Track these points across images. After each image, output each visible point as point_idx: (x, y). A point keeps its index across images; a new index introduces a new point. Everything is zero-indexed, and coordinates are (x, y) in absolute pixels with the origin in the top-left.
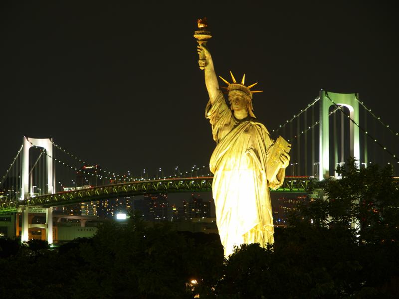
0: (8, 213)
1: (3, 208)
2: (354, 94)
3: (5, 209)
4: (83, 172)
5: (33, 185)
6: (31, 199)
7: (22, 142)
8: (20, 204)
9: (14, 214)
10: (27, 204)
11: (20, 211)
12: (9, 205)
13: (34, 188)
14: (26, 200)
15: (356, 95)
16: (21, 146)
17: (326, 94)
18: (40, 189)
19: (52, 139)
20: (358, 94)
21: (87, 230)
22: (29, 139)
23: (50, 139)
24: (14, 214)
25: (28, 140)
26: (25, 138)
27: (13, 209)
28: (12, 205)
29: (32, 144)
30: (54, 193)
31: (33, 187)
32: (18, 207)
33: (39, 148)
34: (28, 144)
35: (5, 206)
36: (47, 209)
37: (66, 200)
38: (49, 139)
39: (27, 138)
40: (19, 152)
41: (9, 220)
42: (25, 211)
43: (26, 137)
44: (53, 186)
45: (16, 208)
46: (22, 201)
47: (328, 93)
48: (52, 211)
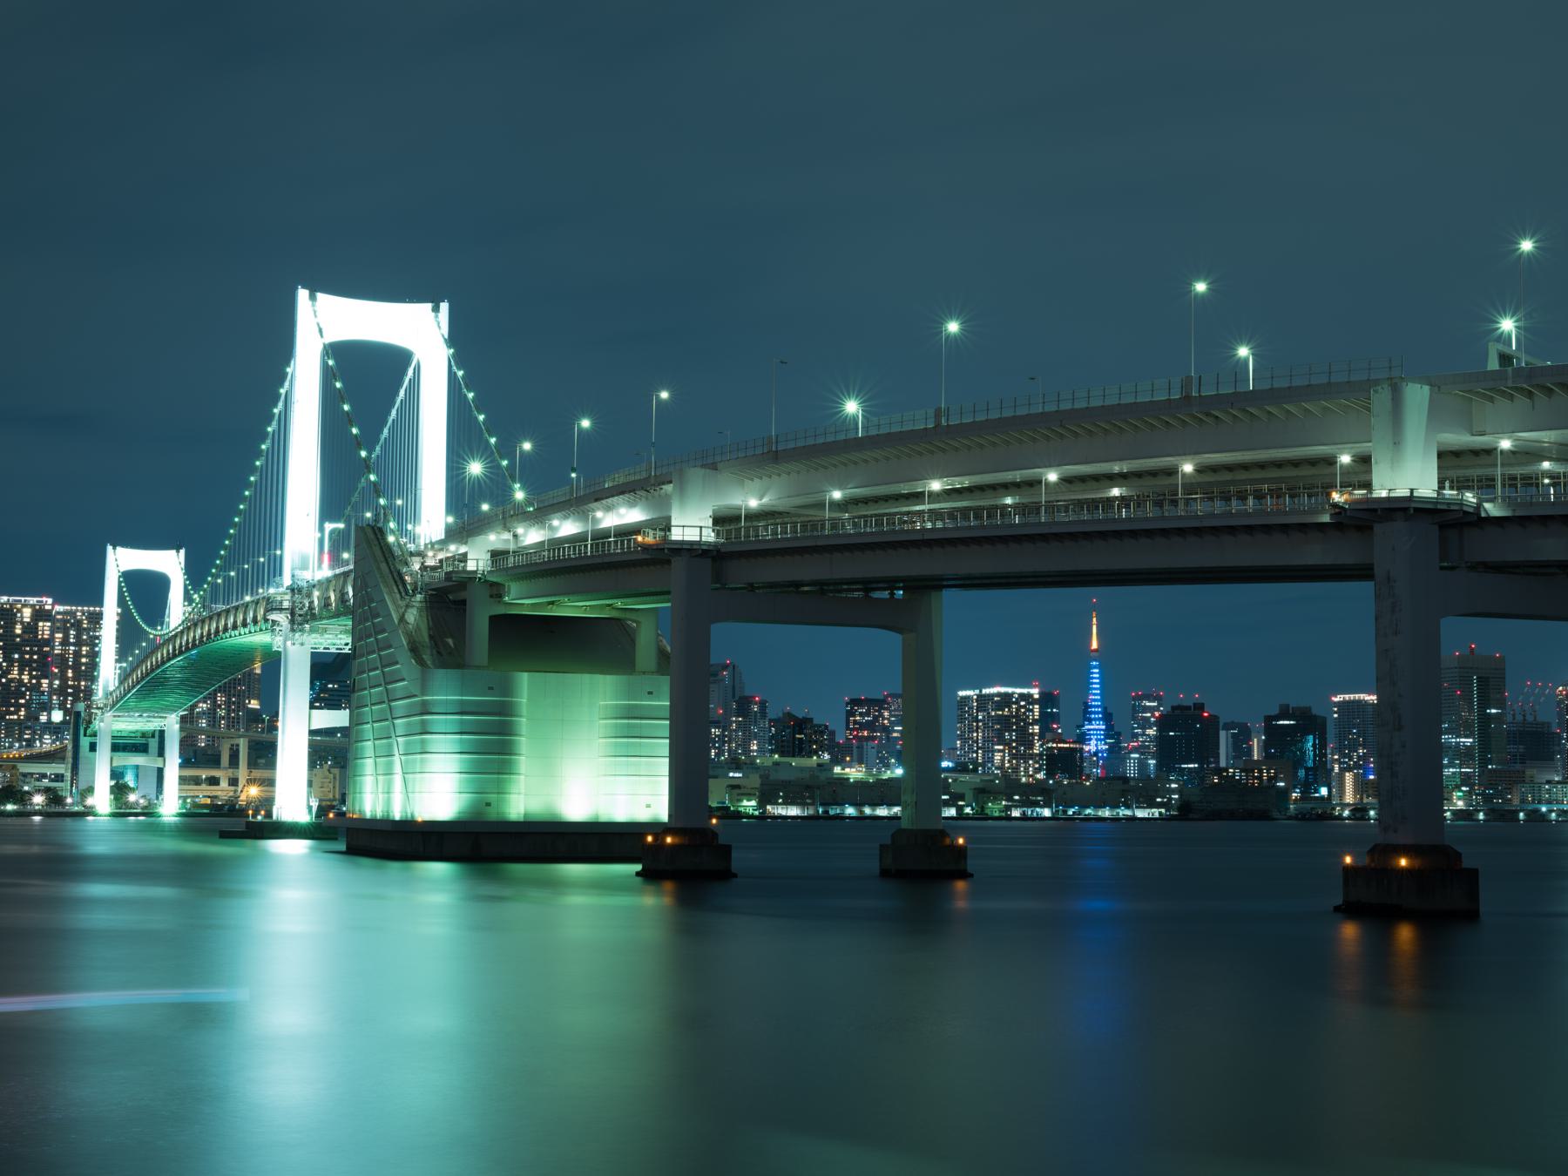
0: (144, 735)
2: (429, 306)
13: (120, 668)
15: (436, 309)
17: (313, 297)
19: (182, 552)
20: (444, 307)
23: (178, 552)
24: (157, 734)
34: (121, 560)
39: (114, 548)
42: (102, 724)
47: (319, 295)
48: (177, 726)
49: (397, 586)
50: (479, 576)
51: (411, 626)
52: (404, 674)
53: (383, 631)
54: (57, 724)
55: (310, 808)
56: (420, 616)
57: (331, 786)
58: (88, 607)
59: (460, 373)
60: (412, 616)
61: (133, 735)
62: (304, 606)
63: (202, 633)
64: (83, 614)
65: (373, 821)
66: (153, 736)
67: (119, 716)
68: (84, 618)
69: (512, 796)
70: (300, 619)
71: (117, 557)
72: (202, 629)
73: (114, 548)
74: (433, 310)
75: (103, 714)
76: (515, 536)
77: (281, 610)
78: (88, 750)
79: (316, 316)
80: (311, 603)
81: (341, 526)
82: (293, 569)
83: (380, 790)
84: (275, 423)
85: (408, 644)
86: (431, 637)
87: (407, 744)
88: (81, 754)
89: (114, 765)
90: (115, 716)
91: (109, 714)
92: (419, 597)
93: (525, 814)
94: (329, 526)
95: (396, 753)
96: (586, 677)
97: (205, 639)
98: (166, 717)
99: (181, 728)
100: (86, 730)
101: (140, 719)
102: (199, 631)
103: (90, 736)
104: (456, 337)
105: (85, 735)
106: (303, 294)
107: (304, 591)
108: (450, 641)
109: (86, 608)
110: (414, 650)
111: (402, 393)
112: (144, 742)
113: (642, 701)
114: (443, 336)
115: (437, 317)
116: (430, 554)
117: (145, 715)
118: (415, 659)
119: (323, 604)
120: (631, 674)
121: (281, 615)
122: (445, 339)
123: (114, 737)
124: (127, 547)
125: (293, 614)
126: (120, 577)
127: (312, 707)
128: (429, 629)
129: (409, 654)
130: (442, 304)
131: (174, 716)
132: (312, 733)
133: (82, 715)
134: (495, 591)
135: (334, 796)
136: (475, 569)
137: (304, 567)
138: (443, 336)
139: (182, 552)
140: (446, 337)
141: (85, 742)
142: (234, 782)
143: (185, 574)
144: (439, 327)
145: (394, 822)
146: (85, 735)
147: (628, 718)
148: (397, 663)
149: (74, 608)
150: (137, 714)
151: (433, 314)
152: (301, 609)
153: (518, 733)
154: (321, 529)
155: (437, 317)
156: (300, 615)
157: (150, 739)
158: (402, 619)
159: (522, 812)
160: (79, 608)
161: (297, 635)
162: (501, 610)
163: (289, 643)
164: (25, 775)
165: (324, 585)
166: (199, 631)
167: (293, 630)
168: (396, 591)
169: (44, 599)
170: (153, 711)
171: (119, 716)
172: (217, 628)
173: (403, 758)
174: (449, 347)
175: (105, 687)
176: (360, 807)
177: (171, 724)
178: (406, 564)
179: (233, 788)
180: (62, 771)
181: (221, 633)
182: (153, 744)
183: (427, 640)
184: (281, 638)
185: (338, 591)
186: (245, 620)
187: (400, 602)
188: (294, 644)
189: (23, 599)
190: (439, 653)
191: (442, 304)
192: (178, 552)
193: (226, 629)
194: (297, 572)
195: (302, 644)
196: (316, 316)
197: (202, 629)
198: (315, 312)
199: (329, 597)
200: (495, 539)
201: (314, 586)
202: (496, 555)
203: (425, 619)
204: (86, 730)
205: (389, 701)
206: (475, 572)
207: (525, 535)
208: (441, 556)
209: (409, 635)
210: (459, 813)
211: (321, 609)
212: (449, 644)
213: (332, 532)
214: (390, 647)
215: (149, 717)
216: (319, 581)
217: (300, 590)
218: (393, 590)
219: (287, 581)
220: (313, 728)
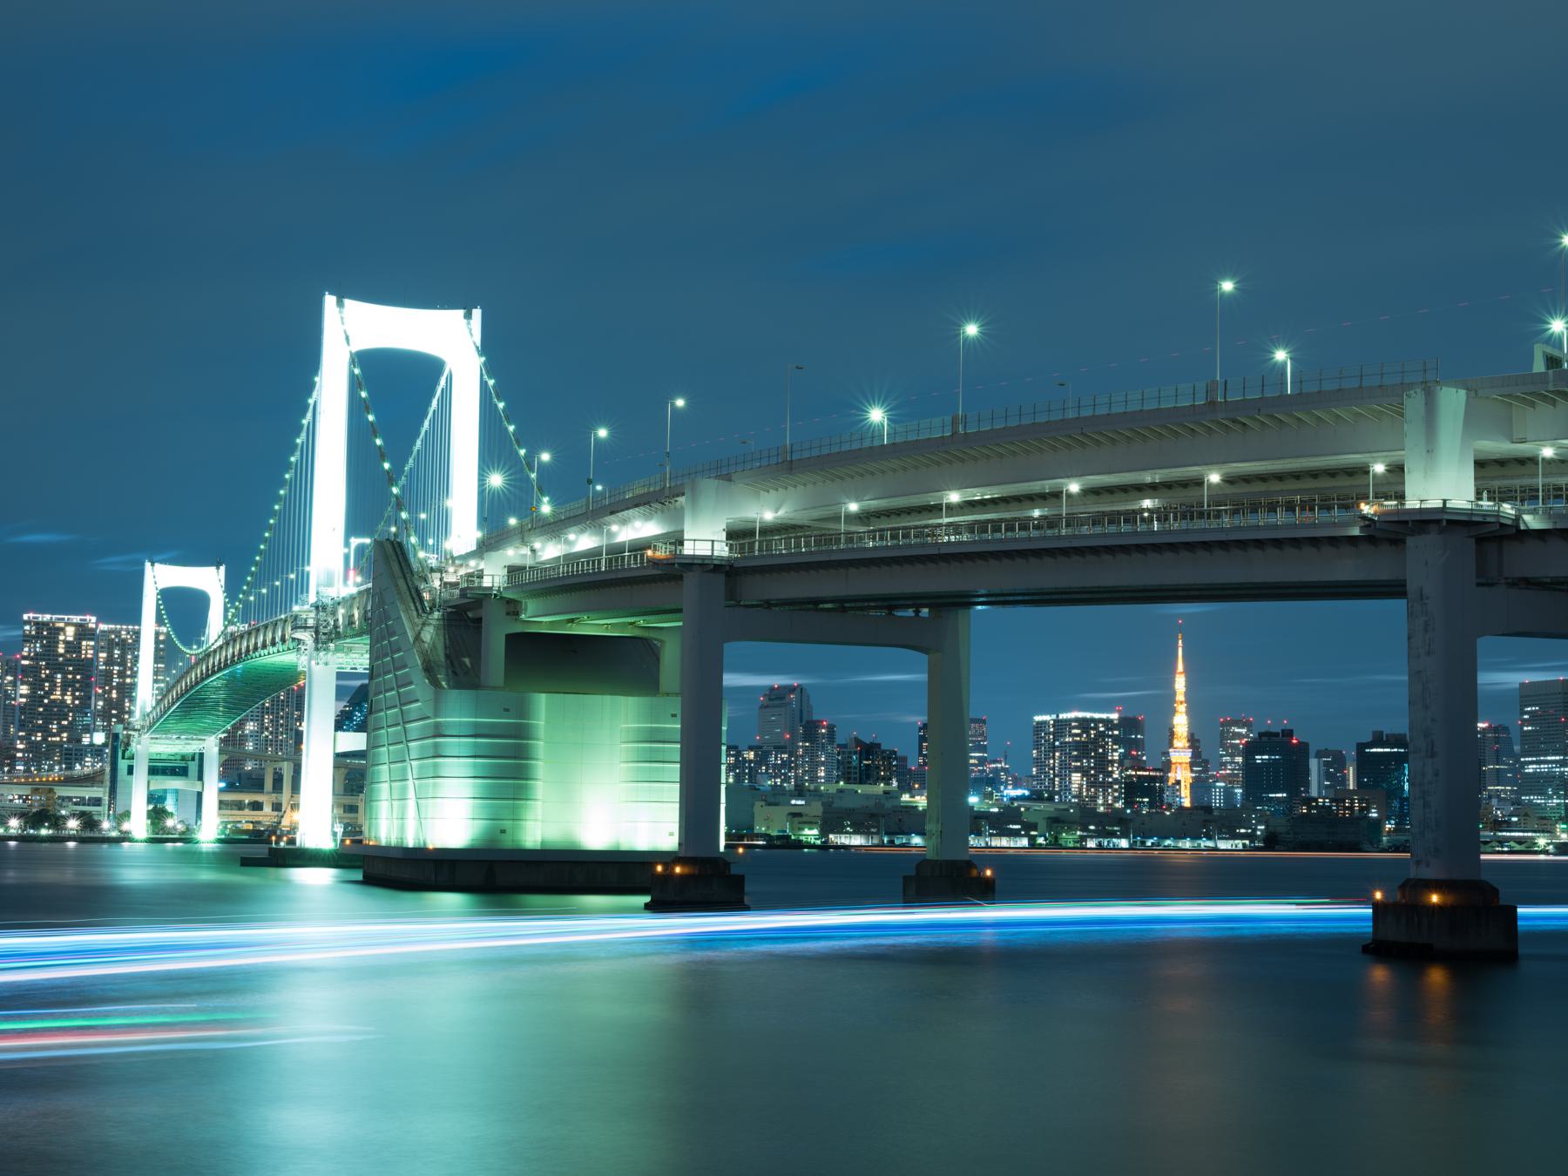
0: (183, 758)
2: (461, 312)
13: (157, 689)
15: (468, 316)
17: (340, 304)
19: (223, 568)
20: (477, 313)
23: (218, 568)
24: (197, 757)
34: (160, 577)
38: (215, 568)
39: (153, 565)
42: (139, 746)
43: (149, 561)
47: (347, 302)
48: (216, 749)
49: (415, 603)
50: (495, 592)
51: (426, 645)
52: (419, 695)
53: (399, 650)
54: (99, 746)
55: (335, 834)
56: (437, 634)
58: (133, 625)
59: (491, 382)
60: (428, 635)
61: (172, 758)
62: (328, 624)
63: (234, 653)
64: (128, 633)
65: (388, 848)
66: (193, 759)
67: (157, 738)
68: (129, 637)
69: (527, 823)
70: (324, 637)
71: (155, 574)
72: (233, 648)
73: (153, 565)
74: (465, 317)
76: (533, 551)
77: (306, 628)
78: (126, 771)
79: (343, 323)
80: (336, 621)
81: (368, 541)
82: (318, 586)
83: (395, 816)
84: (303, 434)
85: (422, 664)
86: (447, 656)
87: (421, 768)
88: (119, 778)
89: (151, 789)
90: (152, 738)
91: (147, 736)
92: (436, 615)
93: (542, 842)
94: (355, 542)
95: (410, 777)
96: (608, 698)
97: (236, 658)
99: (220, 750)
100: (124, 752)
101: (177, 742)
102: (231, 650)
104: (489, 346)
105: (123, 758)
106: (330, 301)
107: (329, 609)
108: (467, 661)
109: (130, 627)
110: (429, 670)
111: (434, 403)
113: (665, 724)
114: (475, 344)
115: (469, 324)
116: (451, 569)
117: (183, 737)
118: (428, 679)
119: (347, 623)
120: (655, 695)
121: (306, 634)
122: (477, 348)
123: (151, 760)
124: (166, 564)
125: (317, 632)
126: (158, 594)
127: (336, 730)
128: (446, 647)
129: (423, 673)
130: (474, 311)
132: (340, 757)
133: (121, 737)
134: (512, 608)
136: (490, 585)
137: (330, 584)
138: (475, 344)
139: (223, 568)
140: (479, 344)
141: (123, 765)
142: (277, 807)
143: (224, 592)
144: (471, 334)
145: (407, 850)
146: (123, 758)
147: (651, 742)
148: (411, 683)
149: (118, 627)
150: (175, 737)
151: (466, 321)
152: (324, 627)
153: (535, 757)
154: (347, 544)
155: (469, 324)
156: (325, 634)
158: (418, 638)
159: (539, 839)
160: (124, 627)
161: (322, 654)
162: (518, 629)
163: (313, 662)
164: (63, 799)
165: (349, 602)
166: (231, 650)
167: (317, 649)
168: (413, 608)
169: (88, 617)
170: (190, 733)
171: (157, 738)
172: (248, 647)
173: (416, 782)
174: (481, 355)
175: (143, 708)
176: (376, 833)
177: (210, 746)
178: (426, 581)
179: (276, 813)
180: (99, 795)
181: (251, 653)
182: (193, 767)
183: (442, 658)
184: (306, 657)
185: (361, 608)
186: (274, 638)
187: (416, 620)
188: (318, 664)
189: (66, 617)
190: (455, 673)
191: (474, 311)
192: (218, 568)
193: (256, 649)
194: (321, 589)
195: (326, 664)
196: (343, 323)
197: (233, 648)
198: (342, 319)
199: (353, 615)
200: (513, 554)
201: (339, 604)
202: (513, 571)
203: (442, 638)
204: (124, 752)
205: (404, 723)
206: (491, 588)
207: (543, 549)
208: (462, 572)
209: (424, 654)
210: (473, 840)
211: (345, 627)
212: (464, 663)
213: (361, 550)
214: (404, 667)
215: (187, 739)
216: (343, 598)
217: (324, 608)
218: (409, 606)
219: (312, 599)
220: (340, 750)
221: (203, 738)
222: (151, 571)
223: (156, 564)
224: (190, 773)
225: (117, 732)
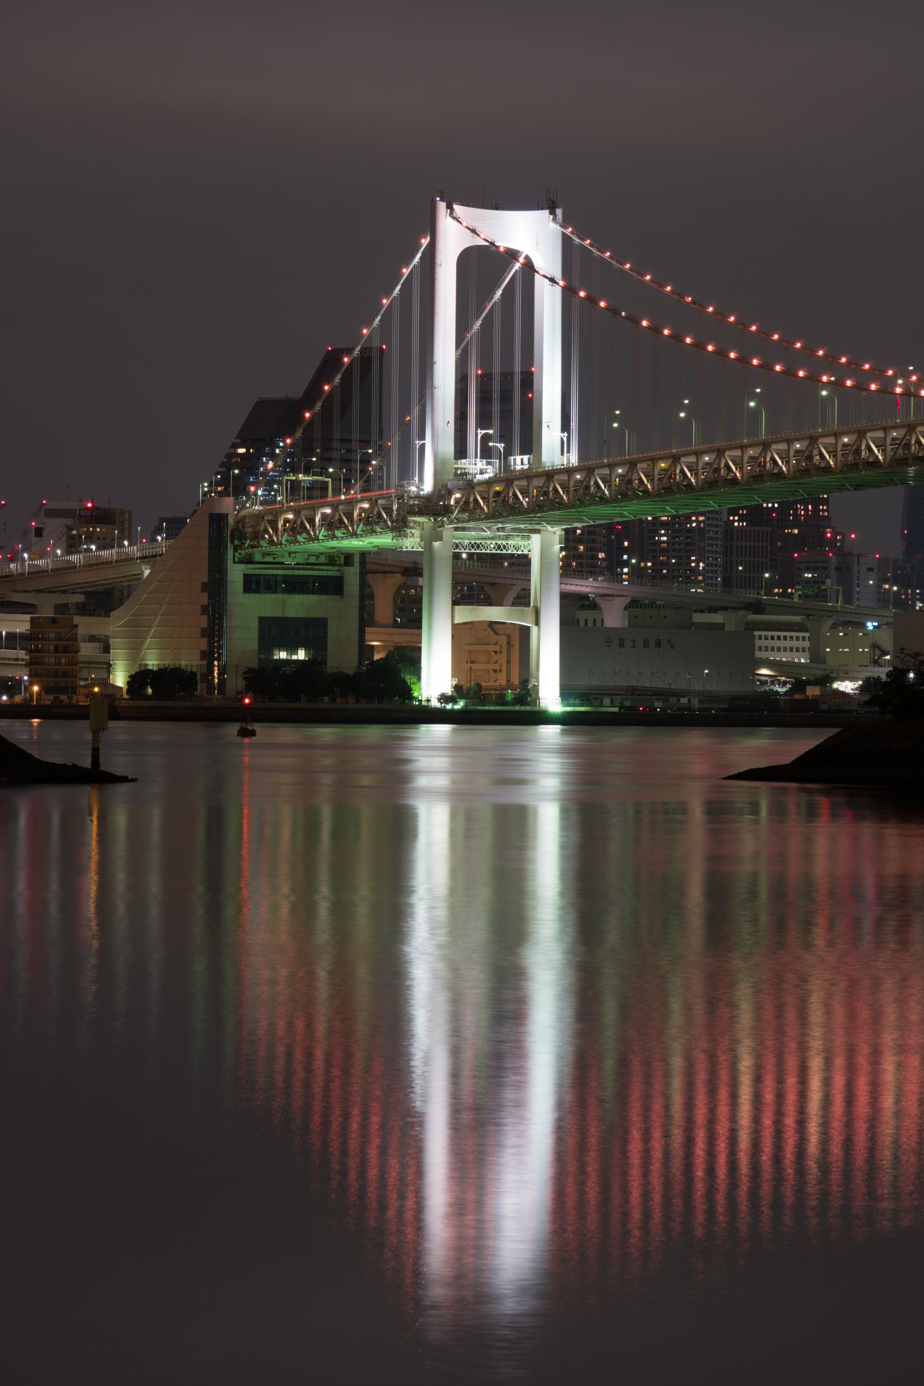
1: (322, 533)
3: (373, 532)
4: (813, 351)
5: (483, 422)
6: (469, 485)
7: (431, 228)
8: (415, 514)
9: (357, 559)
10: (447, 510)
11: (411, 542)
12: (350, 516)
14: (442, 491)
16: (418, 246)
18: (501, 446)
19: (559, 212)
21: (658, 644)
22: (455, 207)
23: (552, 212)
24: (357, 559)
25: (451, 214)
26: (442, 206)
27: (384, 540)
28: (371, 522)
29: (474, 231)
30: (573, 459)
31: (481, 432)
32: (400, 527)
33: (513, 255)
35: (331, 524)
36: (536, 539)
37: (793, 478)
38: (547, 211)
39: (450, 207)
40: (406, 271)
41: (333, 586)
42: (436, 544)
44: (565, 427)
45: (392, 529)
46: (428, 498)
57: (502, 658)
61: (313, 560)
67: (464, 529)
75: (442, 526)
89: (456, 622)
90: (456, 529)
98: (537, 531)
103: (240, 562)
105: (234, 562)
112: (338, 574)
131: (555, 529)
133: (231, 521)
135: (508, 681)
139: (559, 212)
146: (234, 562)
157: (346, 569)
204: (236, 549)
221: (537, 527)
222: (450, 220)
223: (455, 207)
224: (346, 589)
225: (223, 512)
